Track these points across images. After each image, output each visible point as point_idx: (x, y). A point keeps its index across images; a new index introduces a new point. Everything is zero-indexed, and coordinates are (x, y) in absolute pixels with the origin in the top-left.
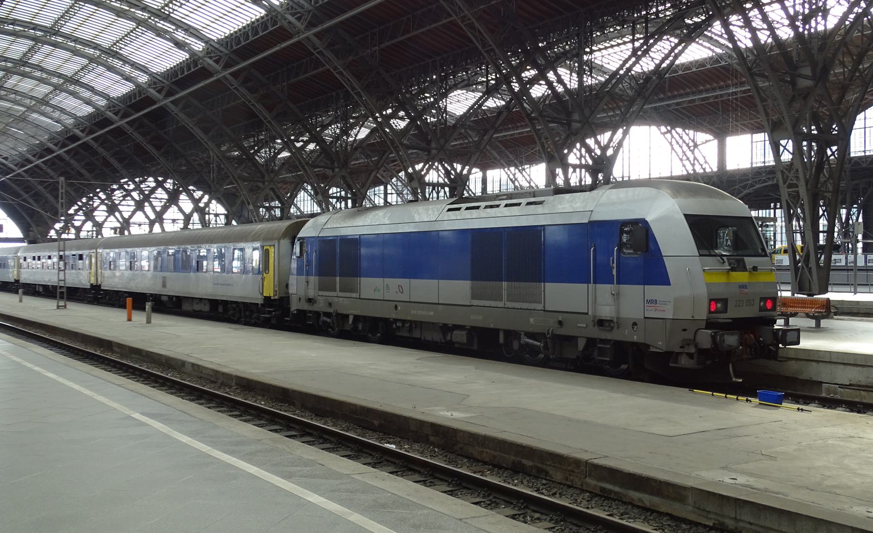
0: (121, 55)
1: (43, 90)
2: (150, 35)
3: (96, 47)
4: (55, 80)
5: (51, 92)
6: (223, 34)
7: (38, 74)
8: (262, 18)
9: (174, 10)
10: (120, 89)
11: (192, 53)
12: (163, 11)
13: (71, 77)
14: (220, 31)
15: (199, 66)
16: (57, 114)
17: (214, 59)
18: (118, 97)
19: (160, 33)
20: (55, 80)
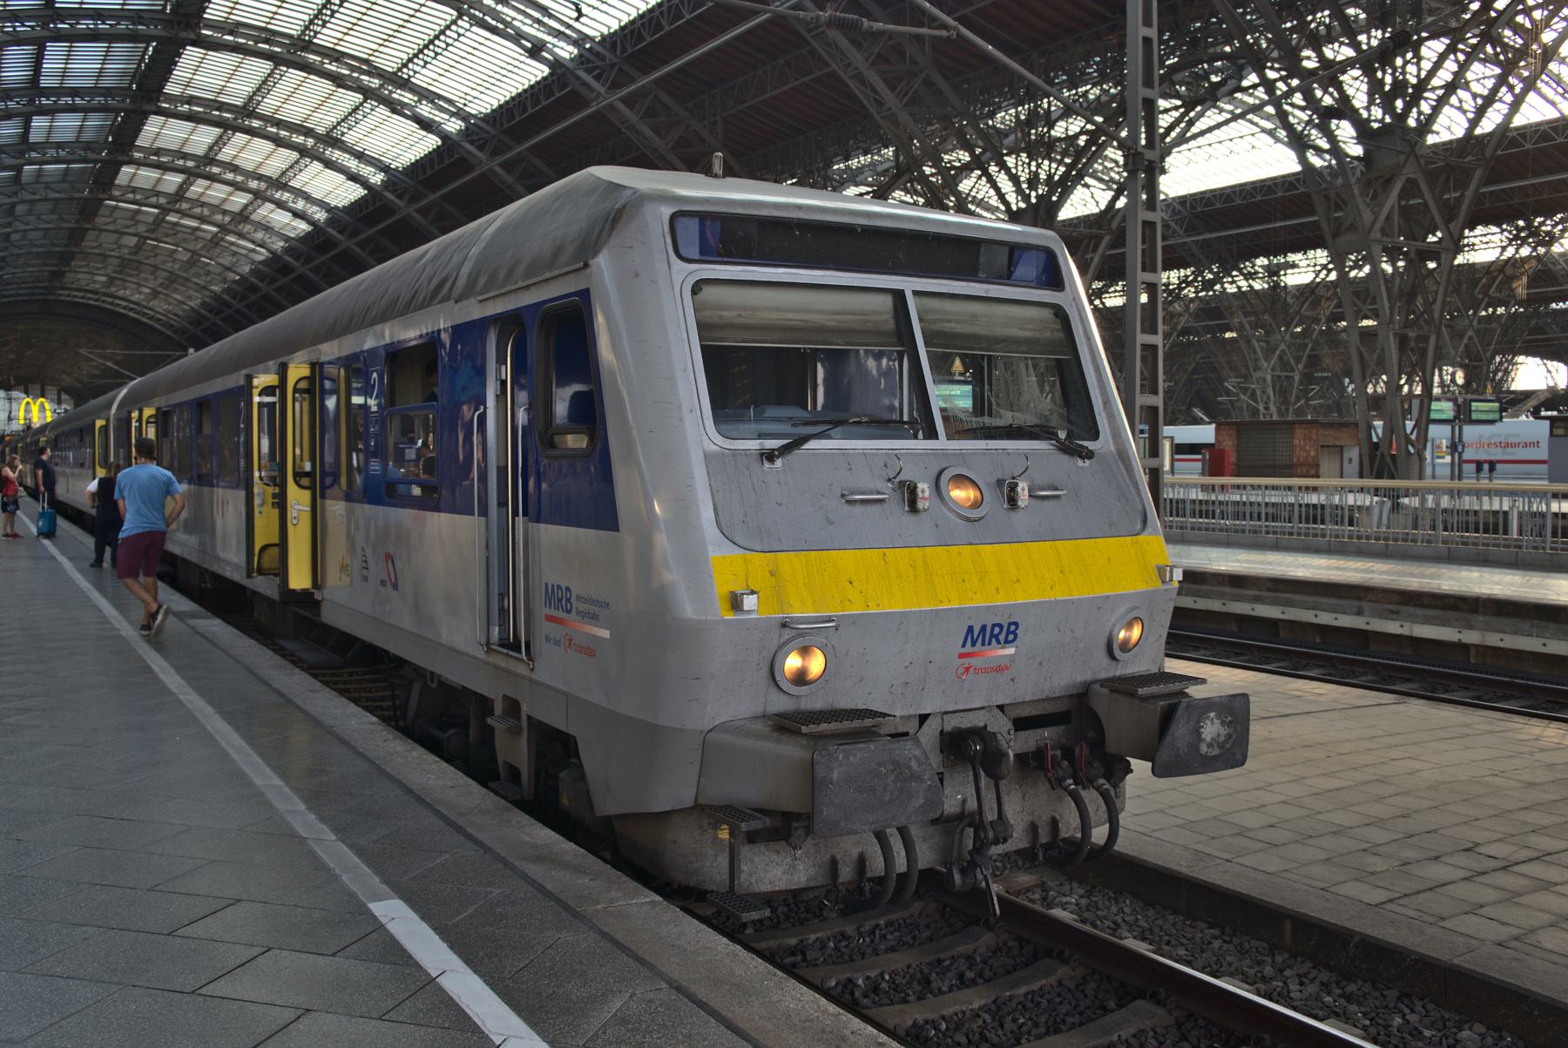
0: (343, 142)
1: (241, 199)
2: (383, 111)
3: (309, 132)
4: (254, 184)
5: (252, 203)
6: (489, 107)
7: (230, 176)
8: (545, 79)
9: (415, 72)
10: (344, 193)
11: (445, 136)
12: (400, 74)
13: (277, 180)
14: (485, 102)
15: (456, 156)
16: (259, 235)
17: (477, 144)
18: (344, 207)
19: (396, 108)
20: (254, 184)
